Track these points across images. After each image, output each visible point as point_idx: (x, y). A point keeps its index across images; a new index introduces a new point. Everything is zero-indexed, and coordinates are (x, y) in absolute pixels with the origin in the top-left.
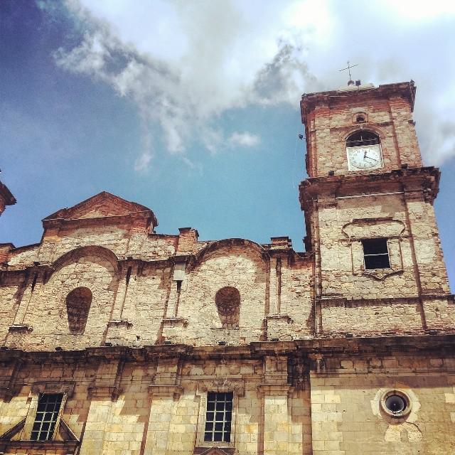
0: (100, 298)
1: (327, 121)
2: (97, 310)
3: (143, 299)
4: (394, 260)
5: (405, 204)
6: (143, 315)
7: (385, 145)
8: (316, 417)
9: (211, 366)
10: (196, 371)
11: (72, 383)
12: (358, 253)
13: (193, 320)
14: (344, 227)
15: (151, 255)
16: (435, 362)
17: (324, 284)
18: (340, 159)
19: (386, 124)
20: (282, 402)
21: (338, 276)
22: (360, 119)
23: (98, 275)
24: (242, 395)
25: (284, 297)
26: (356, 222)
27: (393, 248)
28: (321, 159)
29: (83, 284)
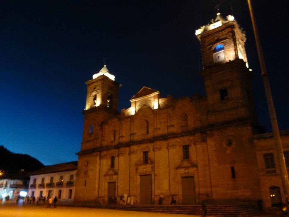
9: (182, 138)
12: (218, 96)
24: (191, 145)
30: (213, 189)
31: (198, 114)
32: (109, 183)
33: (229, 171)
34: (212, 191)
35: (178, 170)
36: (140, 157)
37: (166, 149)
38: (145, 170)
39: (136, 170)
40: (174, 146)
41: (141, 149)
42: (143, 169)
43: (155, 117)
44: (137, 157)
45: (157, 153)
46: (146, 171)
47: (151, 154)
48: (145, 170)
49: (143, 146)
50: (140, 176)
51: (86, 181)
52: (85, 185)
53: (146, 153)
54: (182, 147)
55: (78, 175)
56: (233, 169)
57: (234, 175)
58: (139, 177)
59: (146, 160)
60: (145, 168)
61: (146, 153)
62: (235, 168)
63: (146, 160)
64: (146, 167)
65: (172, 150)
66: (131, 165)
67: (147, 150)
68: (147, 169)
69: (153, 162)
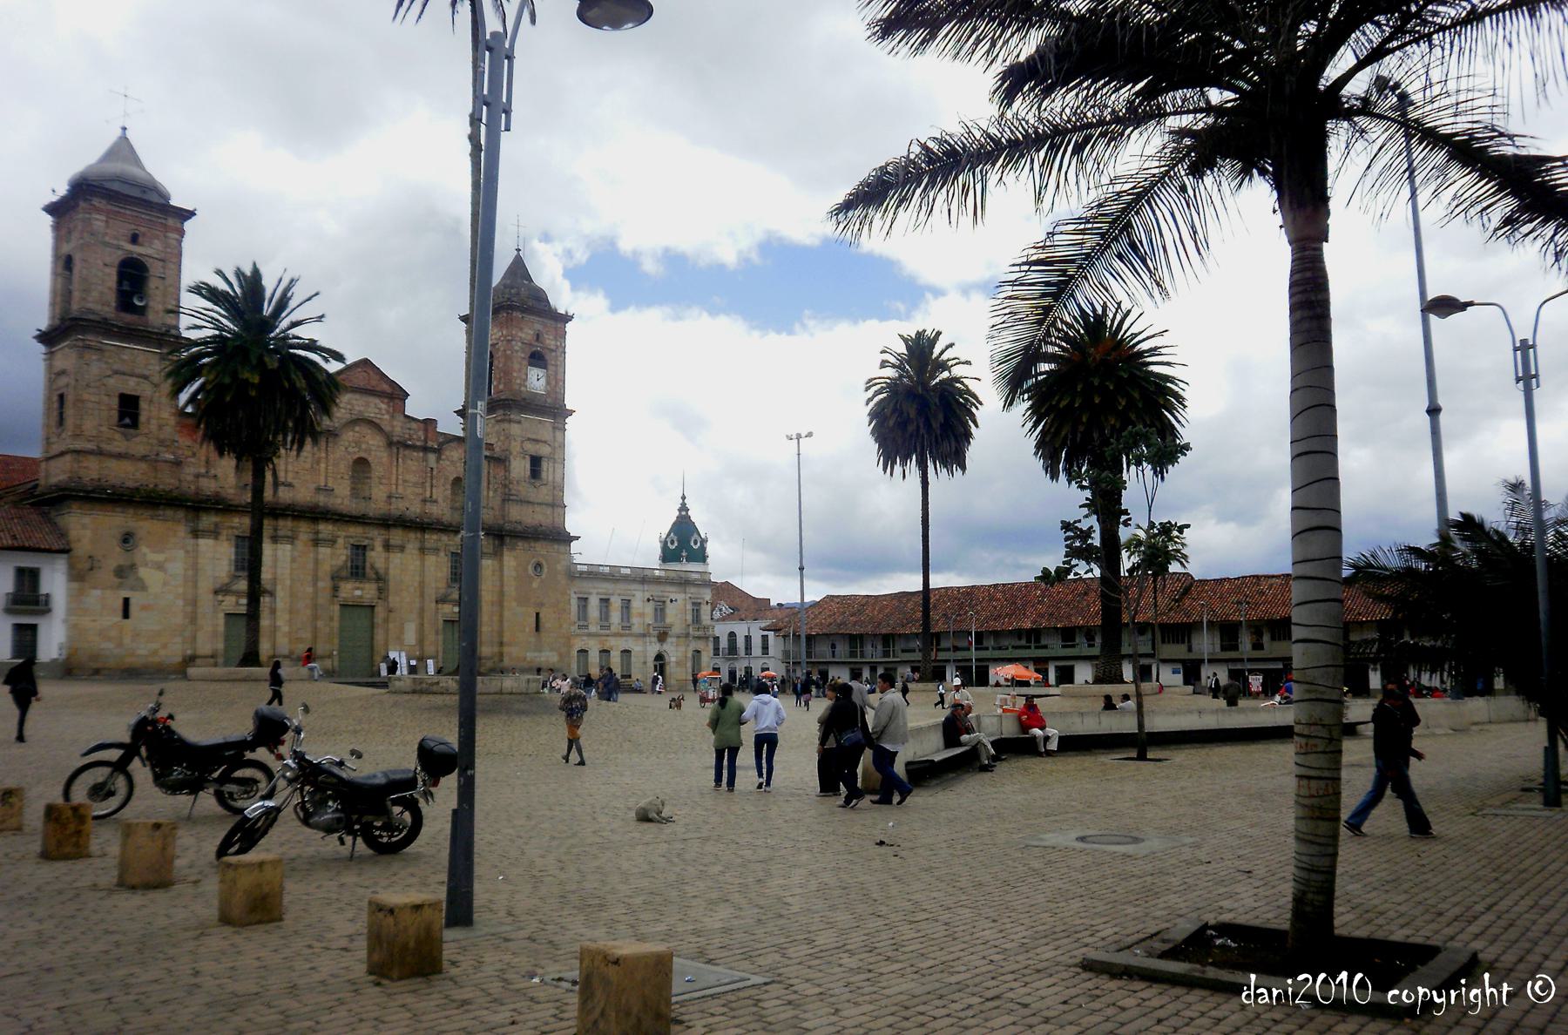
0: (377, 470)
1: (520, 334)
2: (377, 480)
3: (408, 477)
4: (544, 475)
5: (554, 432)
6: (409, 491)
7: (550, 372)
8: (506, 572)
9: (452, 535)
10: (444, 538)
11: (372, 539)
13: (440, 500)
14: (522, 442)
15: (407, 436)
16: (556, 546)
17: (511, 486)
18: (524, 377)
19: (553, 351)
20: (490, 562)
21: (518, 482)
22: (538, 337)
23: (374, 448)
25: (491, 494)
26: (529, 439)
27: (544, 465)
28: (515, 374)
29: (362, 455)
30: (506, 649)
31: (491, 494)
32: (228, 615)
33: (534, 619)
34: (501, 654)
35: (440, 606)
36: (344, 558)
37: (416, 552)
38: (358, 593)
39: (335, 589)
40: (436, 550)
41: (346, 537)
42: (351, 591)
43: (395, 456)
44: (335, 557)
45: (396, 558)
46: (361, 597)
47: (376, 557)
48: (358, 593)
49: (355, 531)
50: (343, 606)
51: (126, 601)
52: (126, 615)
53: (360, 550)
54: (450, 555)
55: (78, 576)
56: (537, 614)
57: (537, 628)
58: (337, 608)
59: (357, 569)
60: (358, 589)
61: (360, 550)
62: (541, 615)
63: (357, 569)
64: (361, 585)
65: (431, 560)
66: (320, 574)
67: (366, 542)
68: (363, 592)
69: (381, 579)
